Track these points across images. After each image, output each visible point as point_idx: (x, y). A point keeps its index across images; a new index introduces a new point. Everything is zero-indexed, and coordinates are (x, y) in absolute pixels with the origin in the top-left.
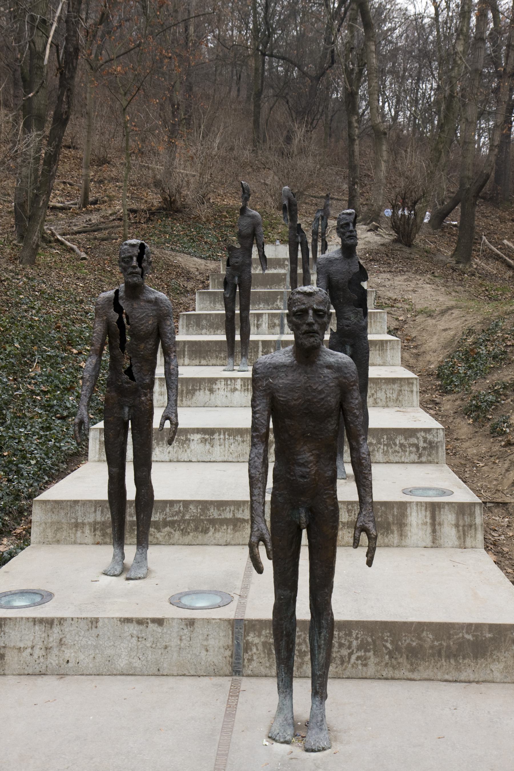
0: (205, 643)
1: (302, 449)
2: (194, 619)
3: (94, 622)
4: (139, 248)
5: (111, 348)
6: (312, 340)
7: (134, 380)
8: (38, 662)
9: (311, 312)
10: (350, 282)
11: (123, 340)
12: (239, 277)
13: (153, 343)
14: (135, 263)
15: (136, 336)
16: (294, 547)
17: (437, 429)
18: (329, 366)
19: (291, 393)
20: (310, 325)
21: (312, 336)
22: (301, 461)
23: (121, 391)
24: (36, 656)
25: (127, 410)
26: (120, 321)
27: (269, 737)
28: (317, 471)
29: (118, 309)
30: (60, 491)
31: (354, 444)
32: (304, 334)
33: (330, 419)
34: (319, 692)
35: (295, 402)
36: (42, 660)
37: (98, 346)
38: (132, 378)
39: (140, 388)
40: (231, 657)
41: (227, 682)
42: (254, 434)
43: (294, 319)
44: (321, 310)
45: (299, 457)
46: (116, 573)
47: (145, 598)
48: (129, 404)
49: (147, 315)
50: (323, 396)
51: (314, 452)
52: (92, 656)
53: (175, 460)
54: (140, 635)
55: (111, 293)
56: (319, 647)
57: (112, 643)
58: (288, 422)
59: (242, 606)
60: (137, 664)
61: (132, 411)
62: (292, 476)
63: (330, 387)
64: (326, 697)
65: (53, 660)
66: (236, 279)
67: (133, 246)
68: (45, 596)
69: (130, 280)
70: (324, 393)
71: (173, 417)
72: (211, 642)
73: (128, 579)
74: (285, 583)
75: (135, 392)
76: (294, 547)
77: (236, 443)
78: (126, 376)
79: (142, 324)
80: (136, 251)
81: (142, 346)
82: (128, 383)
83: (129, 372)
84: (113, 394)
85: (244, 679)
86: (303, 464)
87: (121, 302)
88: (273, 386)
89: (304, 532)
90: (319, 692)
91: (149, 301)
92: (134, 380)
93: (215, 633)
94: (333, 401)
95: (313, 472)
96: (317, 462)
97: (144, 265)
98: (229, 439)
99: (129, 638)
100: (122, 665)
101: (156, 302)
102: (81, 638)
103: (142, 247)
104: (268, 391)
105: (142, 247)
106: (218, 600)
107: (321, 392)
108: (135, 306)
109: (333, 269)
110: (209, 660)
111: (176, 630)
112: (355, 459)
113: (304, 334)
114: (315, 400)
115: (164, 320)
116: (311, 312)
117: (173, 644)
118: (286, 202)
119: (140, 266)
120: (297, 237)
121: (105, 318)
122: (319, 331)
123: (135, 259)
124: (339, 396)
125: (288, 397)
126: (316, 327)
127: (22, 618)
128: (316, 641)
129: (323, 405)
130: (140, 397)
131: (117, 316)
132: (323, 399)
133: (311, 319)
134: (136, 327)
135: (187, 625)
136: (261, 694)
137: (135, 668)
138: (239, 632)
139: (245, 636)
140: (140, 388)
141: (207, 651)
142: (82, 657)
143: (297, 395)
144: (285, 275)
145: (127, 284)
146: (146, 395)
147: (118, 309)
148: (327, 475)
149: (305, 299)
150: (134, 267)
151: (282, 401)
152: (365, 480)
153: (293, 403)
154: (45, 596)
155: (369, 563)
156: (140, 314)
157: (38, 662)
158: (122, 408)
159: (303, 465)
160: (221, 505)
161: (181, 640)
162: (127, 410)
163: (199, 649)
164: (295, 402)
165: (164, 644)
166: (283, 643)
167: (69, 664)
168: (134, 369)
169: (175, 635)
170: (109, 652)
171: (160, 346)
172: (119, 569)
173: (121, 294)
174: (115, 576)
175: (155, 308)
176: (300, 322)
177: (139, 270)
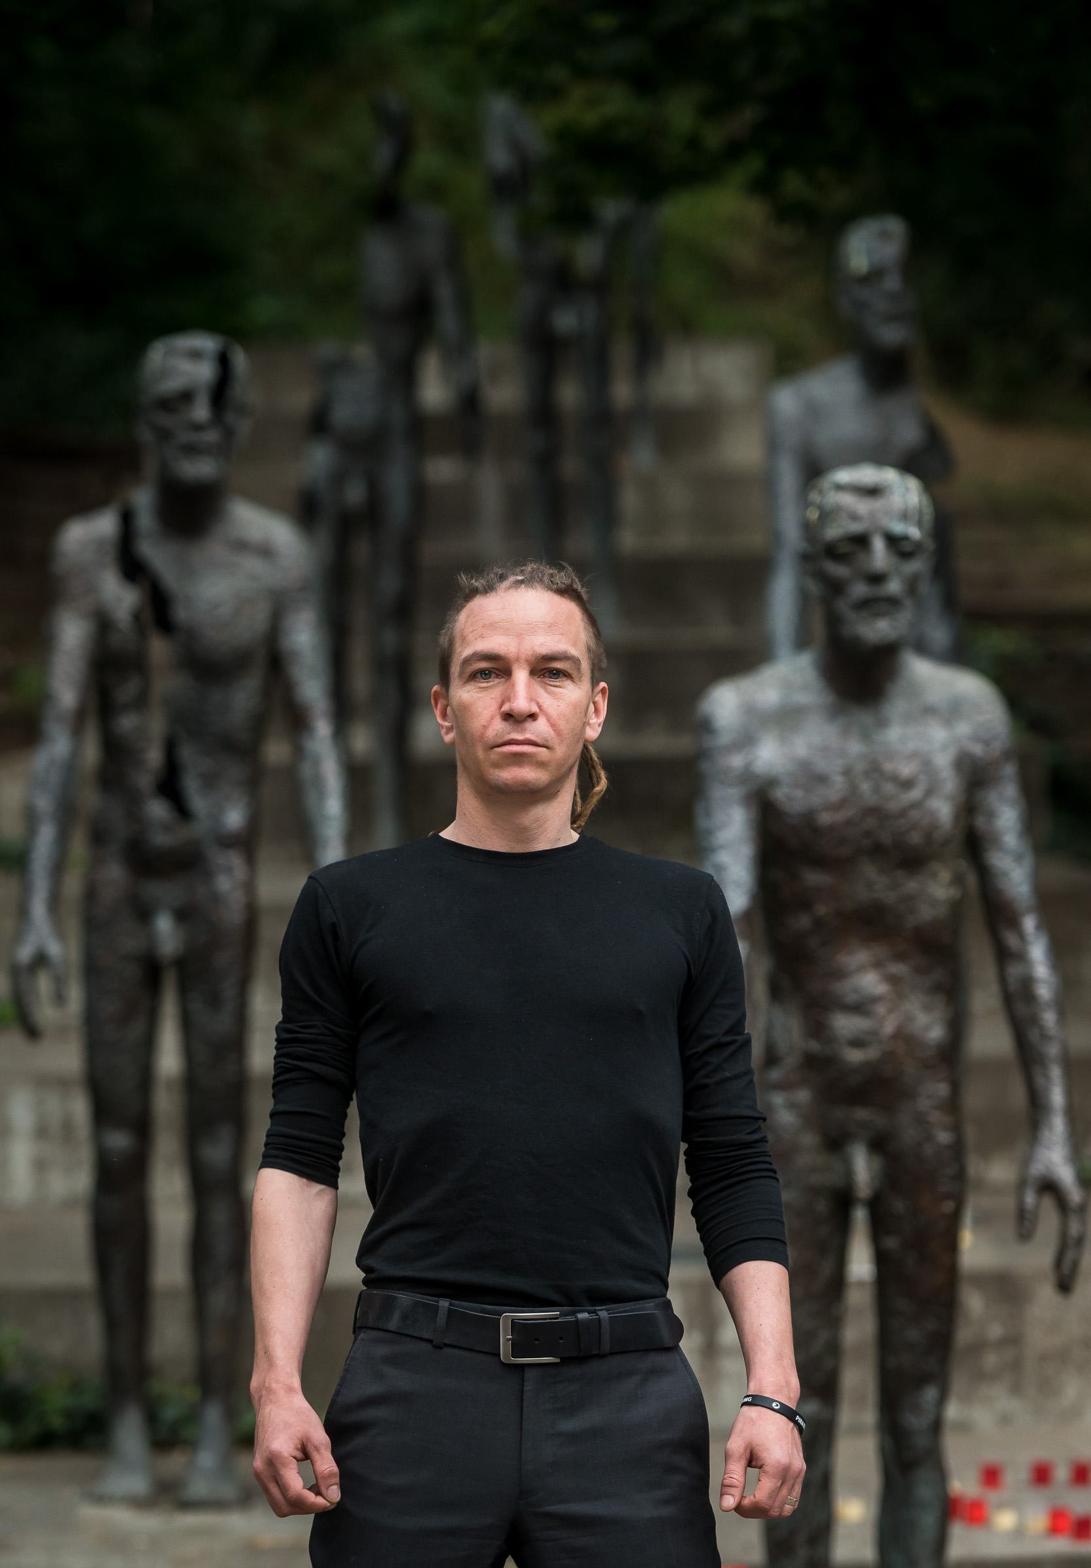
9: (879, 545)
14: (201, 411)
23: (146, 862)
80: (203, 372)
89: (860, 1216)
94: (943, 810)
97: (230, 418)
107: (908, 784)
116: (879, 545)
126: (894, 587)
149: (863, 506)
150: (198, 427)
153: (825, 819)
168: (191, 785)
173: (146, 520)
177: (211, 436)
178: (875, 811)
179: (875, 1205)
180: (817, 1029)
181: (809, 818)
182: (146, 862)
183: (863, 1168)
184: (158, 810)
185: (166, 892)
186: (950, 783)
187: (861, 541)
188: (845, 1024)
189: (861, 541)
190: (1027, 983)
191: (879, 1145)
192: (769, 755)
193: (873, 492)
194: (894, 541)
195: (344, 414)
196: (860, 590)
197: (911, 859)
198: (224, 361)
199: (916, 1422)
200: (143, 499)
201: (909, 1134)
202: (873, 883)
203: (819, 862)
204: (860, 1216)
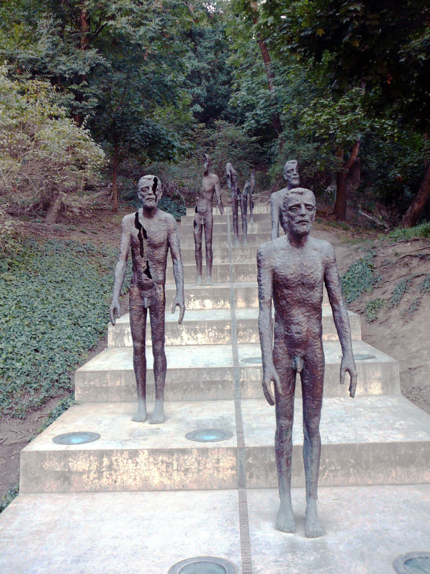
0: (216, 466)
1: (297, 312)
2: (208, 449)
3: (134, 454)
4: (154, 181)
5: (134, 255)
6: (305, 227)
7: (151, 278)
8: (94, 482)
9: (303, 206)
11: (142, 249)
12: (204, 219)
13: (165, 250)
14: (151, 191)
16: (291, 387)
17: (354, 316)
19: (288, 269)
20: (303, 215)
21: (304, 224)
22: (296, 321)
23: (142, 287)
24: (91, 478)
26: (139, 235)
27: (277, 529)
28: (308, 328)
29: (138, 225)
30: (96, 364)
31: (336, 306)
32: (298, 223)
33: (317, 288)
34: (311, 494)
35: (291, 276)
36: (96, 481)
38: (150, 277)
39: (155, 284)
40: (237, 475)
41: (236, 493)
42: (262, 301)
43: (290, 212)
44: (309, 205)
45: (294, 318)
46: (142, 419)
47: (169, 434)
48: (147, 296)
49: (159, 230)
50: (312, 270)
51: (306, 314)
52: (134, 477)
53: (170, 344)
54: (168, 461)
56: (312, 461)
57: (148, 468)
58: (285, 291)
59: (240, 439)
60: (167, 482)
61: (150, 301)
62: (290, 333)
63: (317, 264)
64: (317, 498)
65: (104, 481)
66: (203, 220)
67: (150, 179)
68: (94, 437)
69: (147, 204)
70: (312, 268)
71: (181, 304)
72: (221, 464)
73: (151, 424)
74: (284, 414)
76: (291, 387)
77: (213, 331)
78: (145, 275)
79: (156, 236)
80: (152, 183)
81: (156, 252)
82: (146, 280)
83: (147, 272)
85: (248, 491)
86: (298, 323)
87: (140, 221)
88: (273, 264)
89: (298, 376)
90: (311, 494)
92: (151, 278)
93: (224, 458)
94: (319, 274)
95: (305, 329)
96: (308, 321)
97: (156, 193)
98: (208, 329)
99: (160, 463)
100: (155, 483)
102: (124, 464)
104: (271, 269)
108: (151, 223)
110: (221, 477)
111: (194, 456)
112: (337, 318)
113: (298, 223)
114: (306, 274)
115: (172, 233)
116: (303, 206)
117: (193, 467)
118: (229, 173)
119: (155, 194)
120: (237, 196)
121: (129, 233)
122: (310, 221)
123: (151, 188)
124: (323, 271)
125: (286, 272)
126: (307, 218)
127: (80, 451)
128: (309, 457)
129: (312, 277)
130: (155, 290)
131: (138, 231)
132: (312, 273)
134: (152, 239)
135: (202, 453)
136: (264, 498)
137: (166, 485)
138: (242, 456)
139: (246, 460)
140: (155, 284)
141: (218, 471)
142: (125, 478)
143: (292, 270)
144: (227, 225)
146: (160, 289)
147: (138, 225)
148: (315, 331)
149: (298, 197)
150: (150, 194)
151: (282, 275)
152: (345, 333)
154: (94, 437)
155: (352, 395)
157: (94, 482)
158: (142, 298)
160: (210, 371)
161: (199, 464)
162: (146, 299)
163: (212, 470)
164: (291, 276)
165: (186, 467)
166: (283, 461)
167: (117, 484)
168: (151, 270)
169: (193, 460)
170: (147, 474)
171: (169, 253)
172: (144, 417)
173: (141, 215)
174: (141, 421)
175: (165, 224)
176: (294, 214)
177: (153, 196)
179: (302, 374)
180: (288, 329)
183: (300, 364)
184: (144, 276)
185: (148, 293)
187: (299, 206)
191: (304, 358)
193: (301, 193)
194: (306, 205)
196: (299, 218)
197: (312, 287)
198: (155, 180)
199: (312, 426)
200: (141, 211)
201: (310, 356)
202: (300, 293)
203: (287, 288)
204: (298, 376)
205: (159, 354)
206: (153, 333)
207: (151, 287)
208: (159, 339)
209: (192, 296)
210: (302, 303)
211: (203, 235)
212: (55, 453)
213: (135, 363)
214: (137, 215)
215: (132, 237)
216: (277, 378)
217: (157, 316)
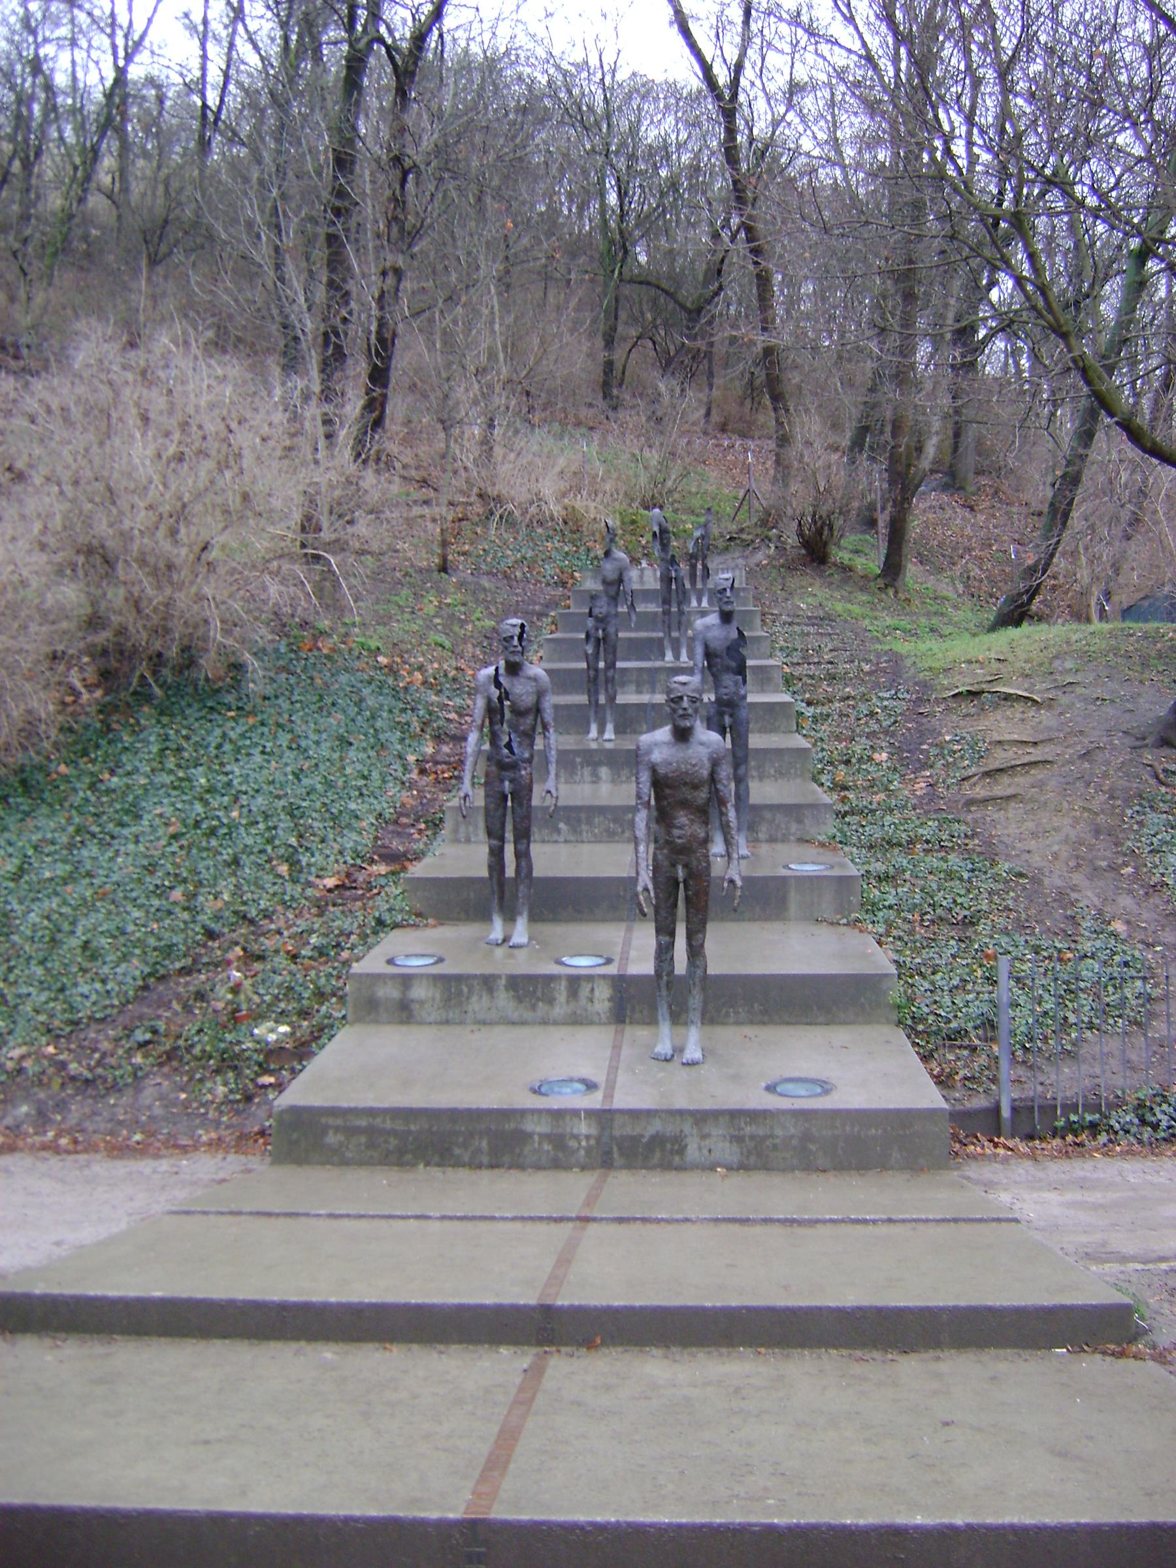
5: (491, 723)
10: (728, 648)
14: (516, 642)
15: (518, 713)
18: (702, 744)
25: (507, 783)
26: (500, 699)
29: (498, 685)
37: (479, 722)
38: (512, 752)
41: (612, 1029)
55: (491, 670)
58: (668, 791)
75: (514, 766)
80: (518, 631)
83: (509, 746)
84: (494, 768)
87: (501, 679)
91: (529, 678)
94: (705, 773)
101: (535, 679)
103: (522, 626)
105: (522, 626)
106: (601, 961)
109: (710, 635)
118: (656, 529)
126: (690, 711)
133: (685, 703)
145: (507, 662)
147: (498, 685)
149: (681, 688)
156: (522, 691)
158: (502, 781)
159: (680, 828)
162: (507, 783)
168: (515, 745)
173: (501, 671)
178: (686, 773)
180: (669, 833)
181: (666, 776)
182: (503, 766)
183: (681, 873)
184: (506, 751)
186: (707, 765)
187: (681, 698)
188: (676, 832)
189: (681, 698)
190: (728, 822)
191: (685, 866)
192: (657, 756)
195: (596, 611)
196: (681, 712)
197: (696, 787)
202: (687, 793)
203: (668, 787)
205: (522, 855)
206: (515, 828)
207: (514, 766)
208: (523, 835)
209: (578, 760)
210: (685, 804)
211: (602, 654)
212: (394, 977)
213: (490, 867)
214: (497, 669)
215: (489, 701)
216: (650, 887)
217: (521, 805)
